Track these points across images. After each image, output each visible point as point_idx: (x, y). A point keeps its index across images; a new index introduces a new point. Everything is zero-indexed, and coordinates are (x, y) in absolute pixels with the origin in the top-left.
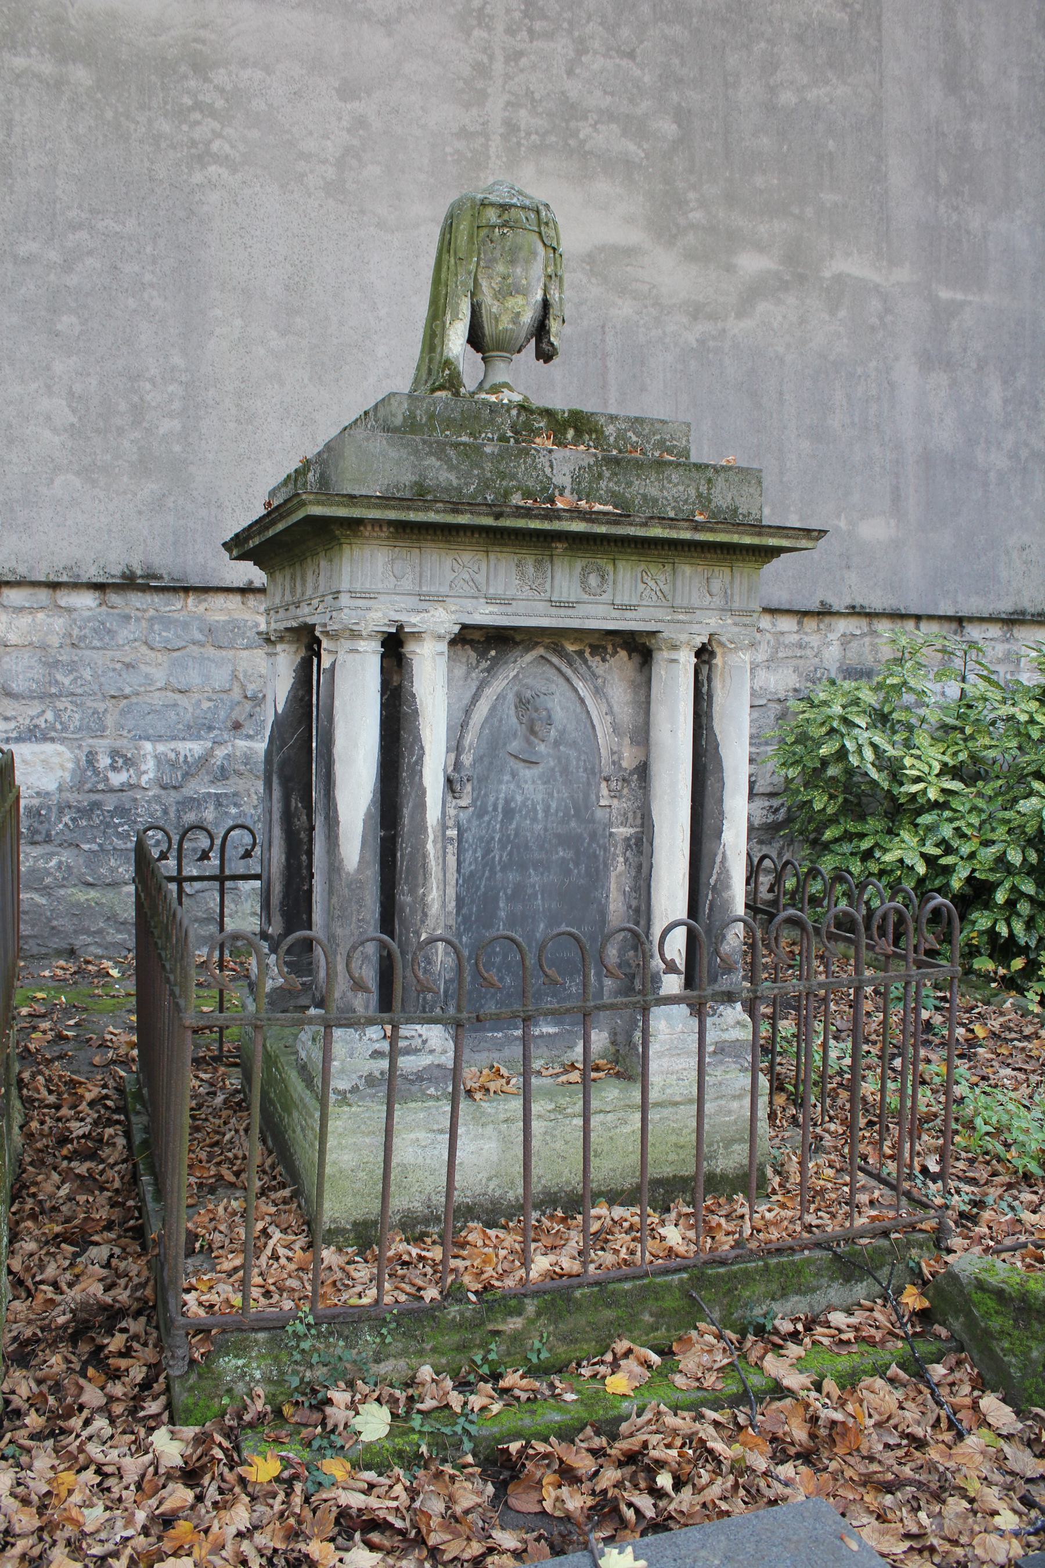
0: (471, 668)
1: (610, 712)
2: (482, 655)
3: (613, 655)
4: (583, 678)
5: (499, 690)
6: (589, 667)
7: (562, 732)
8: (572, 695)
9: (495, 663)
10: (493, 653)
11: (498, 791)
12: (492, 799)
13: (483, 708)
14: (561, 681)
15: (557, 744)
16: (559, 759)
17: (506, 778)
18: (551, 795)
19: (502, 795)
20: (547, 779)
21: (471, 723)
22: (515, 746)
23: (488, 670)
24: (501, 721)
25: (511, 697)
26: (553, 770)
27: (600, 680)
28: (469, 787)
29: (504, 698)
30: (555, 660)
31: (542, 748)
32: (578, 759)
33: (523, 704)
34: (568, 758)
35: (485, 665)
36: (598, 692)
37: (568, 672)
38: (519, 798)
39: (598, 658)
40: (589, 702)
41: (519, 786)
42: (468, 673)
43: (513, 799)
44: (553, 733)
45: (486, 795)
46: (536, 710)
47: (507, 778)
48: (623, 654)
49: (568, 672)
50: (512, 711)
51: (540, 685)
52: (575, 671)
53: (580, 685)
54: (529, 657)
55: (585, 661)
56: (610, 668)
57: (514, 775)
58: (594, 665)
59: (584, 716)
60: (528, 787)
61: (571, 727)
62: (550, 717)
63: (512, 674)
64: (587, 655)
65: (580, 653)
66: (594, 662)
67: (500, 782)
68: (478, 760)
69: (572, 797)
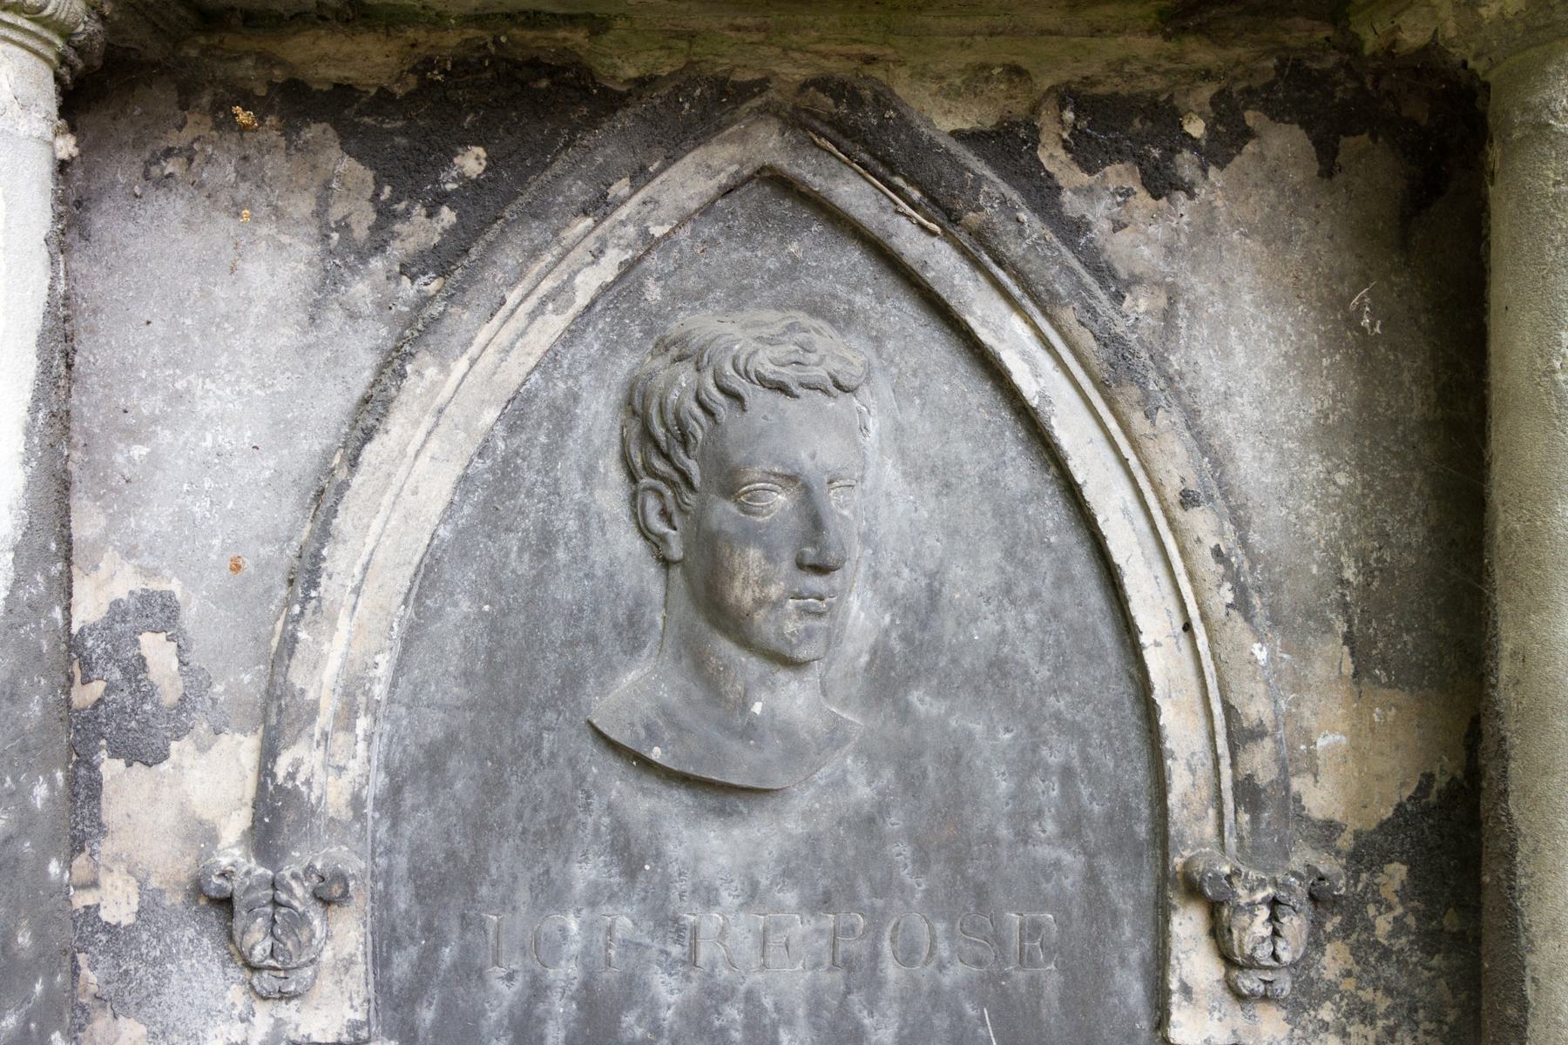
0: (343, 254)
1: (1216, 486)
2: (407, 174)
3: (1218, 151)
4: (1028, 294)
5: (516, 370)
6: (1072, 230)
7: (922, 610)
8: (978, 396)
9: (483, 208)
10: (472, 162)
11: (544, 948)
12: (502, 992)
13: (413, 486)
14: (903, 313)
15: (886, 678)
16: (906, 761)
17: (587, 871)
18: (859, 972)
19: (566, 972)
20: (836, 876)
21: (340, 562)
22: (635, 690)
23: (440, 260)
24: (545, 541)
25: (599, 414)
26: (868, 824)
27: (1141, 303)
28: (346, 935)
29: (562, 417)
30: (855, 194)
31: (792, 700)
32: (1027, 765)
33: (674, 457)
34: (955, 760)
35: (422, 230)
36: (1115, 376)
37: (940, 261)
38: (668, 991)
39: (1119, 174)
40: (1074, 430)
41: (669, 924)
42: (329, 282)
43: (632, 989)
44: (862, 615)
45: (470, 971)
46: (730, 484)
47: (587, 871)
48: (1282, 143)
49: (940, 261)
50: (611, 496)
51: (744, 336)
52: (980, 249)
53: (1010, 336)
54: (688, 181)
55: (1044, 194)
56: (1207, 228)
57: (631, 855)
58: (1099, 214)
59: (1052, 513)
60: (725, 930)
61: (971, 577)
62: (815, 523)
63: (589, 282)
64: (1052, 157)
65: (1008, 145)
66: (1101, 198)
67: (551, 894)
68: (413, 774)
69: (991, 988)
